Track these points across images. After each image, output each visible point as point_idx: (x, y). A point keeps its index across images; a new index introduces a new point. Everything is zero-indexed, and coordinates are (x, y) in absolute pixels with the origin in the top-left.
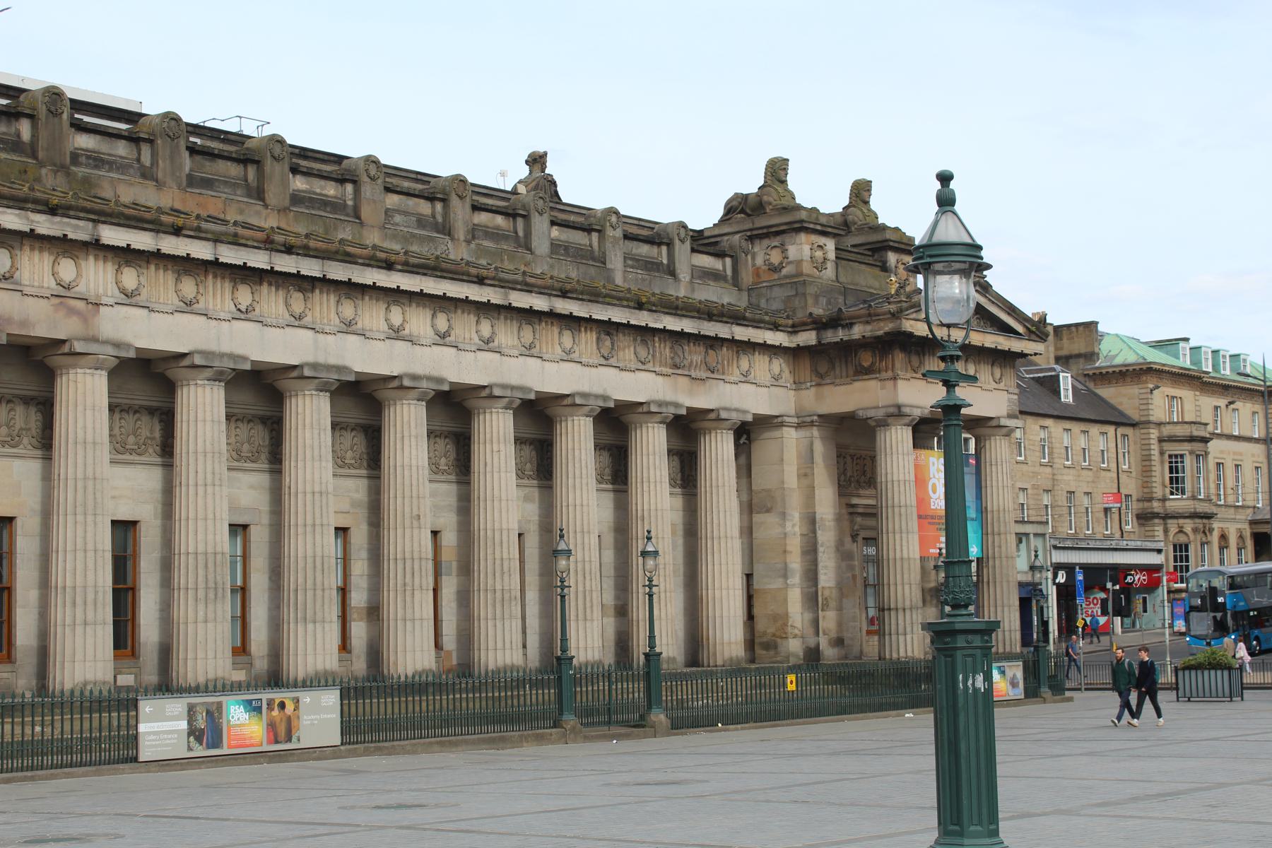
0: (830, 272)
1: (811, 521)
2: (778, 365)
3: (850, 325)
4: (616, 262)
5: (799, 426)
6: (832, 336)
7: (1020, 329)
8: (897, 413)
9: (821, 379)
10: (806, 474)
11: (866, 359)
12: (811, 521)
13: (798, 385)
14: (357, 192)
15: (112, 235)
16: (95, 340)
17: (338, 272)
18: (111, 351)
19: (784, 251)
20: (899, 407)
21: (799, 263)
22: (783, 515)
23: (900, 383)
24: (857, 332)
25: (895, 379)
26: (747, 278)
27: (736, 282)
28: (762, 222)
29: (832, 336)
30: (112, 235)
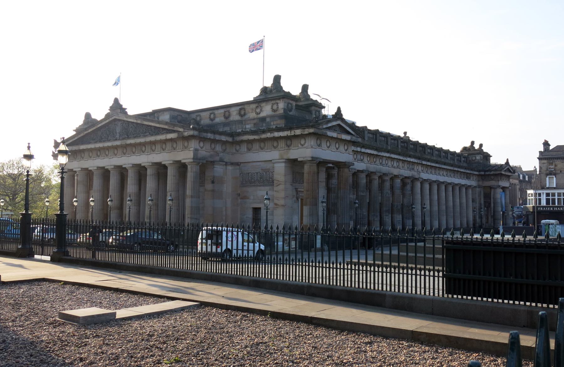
0: (482, 161)
1: (481, 204)
2: (477, 177)
3: (491, 172)
4: (456, 161)
5: (479, 188)
6: (487, 173)
7: (512, 171)
8: (499, 186)
9: (483, 180)
10: (480, 195)
11: (492, 177)
12: (481, 204)
13: (479, 181)
14: (433, 151)
15: (424, 162)
16: (420, 178)
17: (440, 166)
18: (421, 179)
19: (476, 158)
20: (499, 186)
21: (478, 160)
22: (476, 203)
23: (499, 182)
24: (492, 173)
25: (498, 181)
26: (468, 162)
27: (466, 162)
28: (470, 152)
29: (487, 173)
30: (424, 162)
